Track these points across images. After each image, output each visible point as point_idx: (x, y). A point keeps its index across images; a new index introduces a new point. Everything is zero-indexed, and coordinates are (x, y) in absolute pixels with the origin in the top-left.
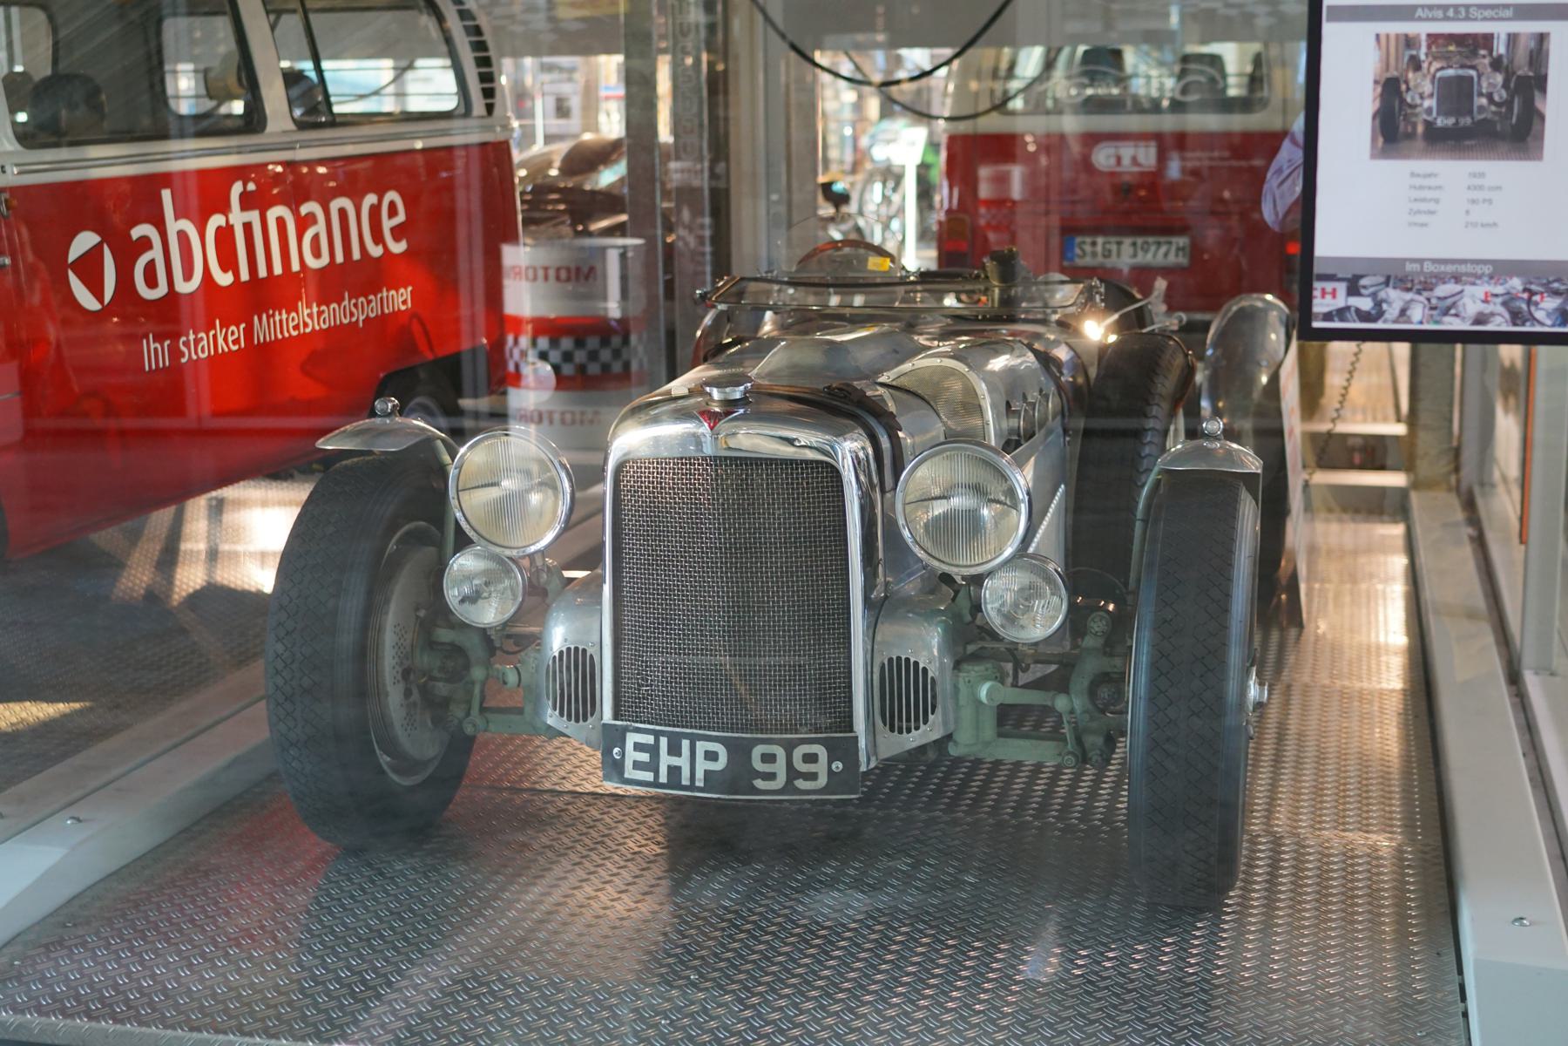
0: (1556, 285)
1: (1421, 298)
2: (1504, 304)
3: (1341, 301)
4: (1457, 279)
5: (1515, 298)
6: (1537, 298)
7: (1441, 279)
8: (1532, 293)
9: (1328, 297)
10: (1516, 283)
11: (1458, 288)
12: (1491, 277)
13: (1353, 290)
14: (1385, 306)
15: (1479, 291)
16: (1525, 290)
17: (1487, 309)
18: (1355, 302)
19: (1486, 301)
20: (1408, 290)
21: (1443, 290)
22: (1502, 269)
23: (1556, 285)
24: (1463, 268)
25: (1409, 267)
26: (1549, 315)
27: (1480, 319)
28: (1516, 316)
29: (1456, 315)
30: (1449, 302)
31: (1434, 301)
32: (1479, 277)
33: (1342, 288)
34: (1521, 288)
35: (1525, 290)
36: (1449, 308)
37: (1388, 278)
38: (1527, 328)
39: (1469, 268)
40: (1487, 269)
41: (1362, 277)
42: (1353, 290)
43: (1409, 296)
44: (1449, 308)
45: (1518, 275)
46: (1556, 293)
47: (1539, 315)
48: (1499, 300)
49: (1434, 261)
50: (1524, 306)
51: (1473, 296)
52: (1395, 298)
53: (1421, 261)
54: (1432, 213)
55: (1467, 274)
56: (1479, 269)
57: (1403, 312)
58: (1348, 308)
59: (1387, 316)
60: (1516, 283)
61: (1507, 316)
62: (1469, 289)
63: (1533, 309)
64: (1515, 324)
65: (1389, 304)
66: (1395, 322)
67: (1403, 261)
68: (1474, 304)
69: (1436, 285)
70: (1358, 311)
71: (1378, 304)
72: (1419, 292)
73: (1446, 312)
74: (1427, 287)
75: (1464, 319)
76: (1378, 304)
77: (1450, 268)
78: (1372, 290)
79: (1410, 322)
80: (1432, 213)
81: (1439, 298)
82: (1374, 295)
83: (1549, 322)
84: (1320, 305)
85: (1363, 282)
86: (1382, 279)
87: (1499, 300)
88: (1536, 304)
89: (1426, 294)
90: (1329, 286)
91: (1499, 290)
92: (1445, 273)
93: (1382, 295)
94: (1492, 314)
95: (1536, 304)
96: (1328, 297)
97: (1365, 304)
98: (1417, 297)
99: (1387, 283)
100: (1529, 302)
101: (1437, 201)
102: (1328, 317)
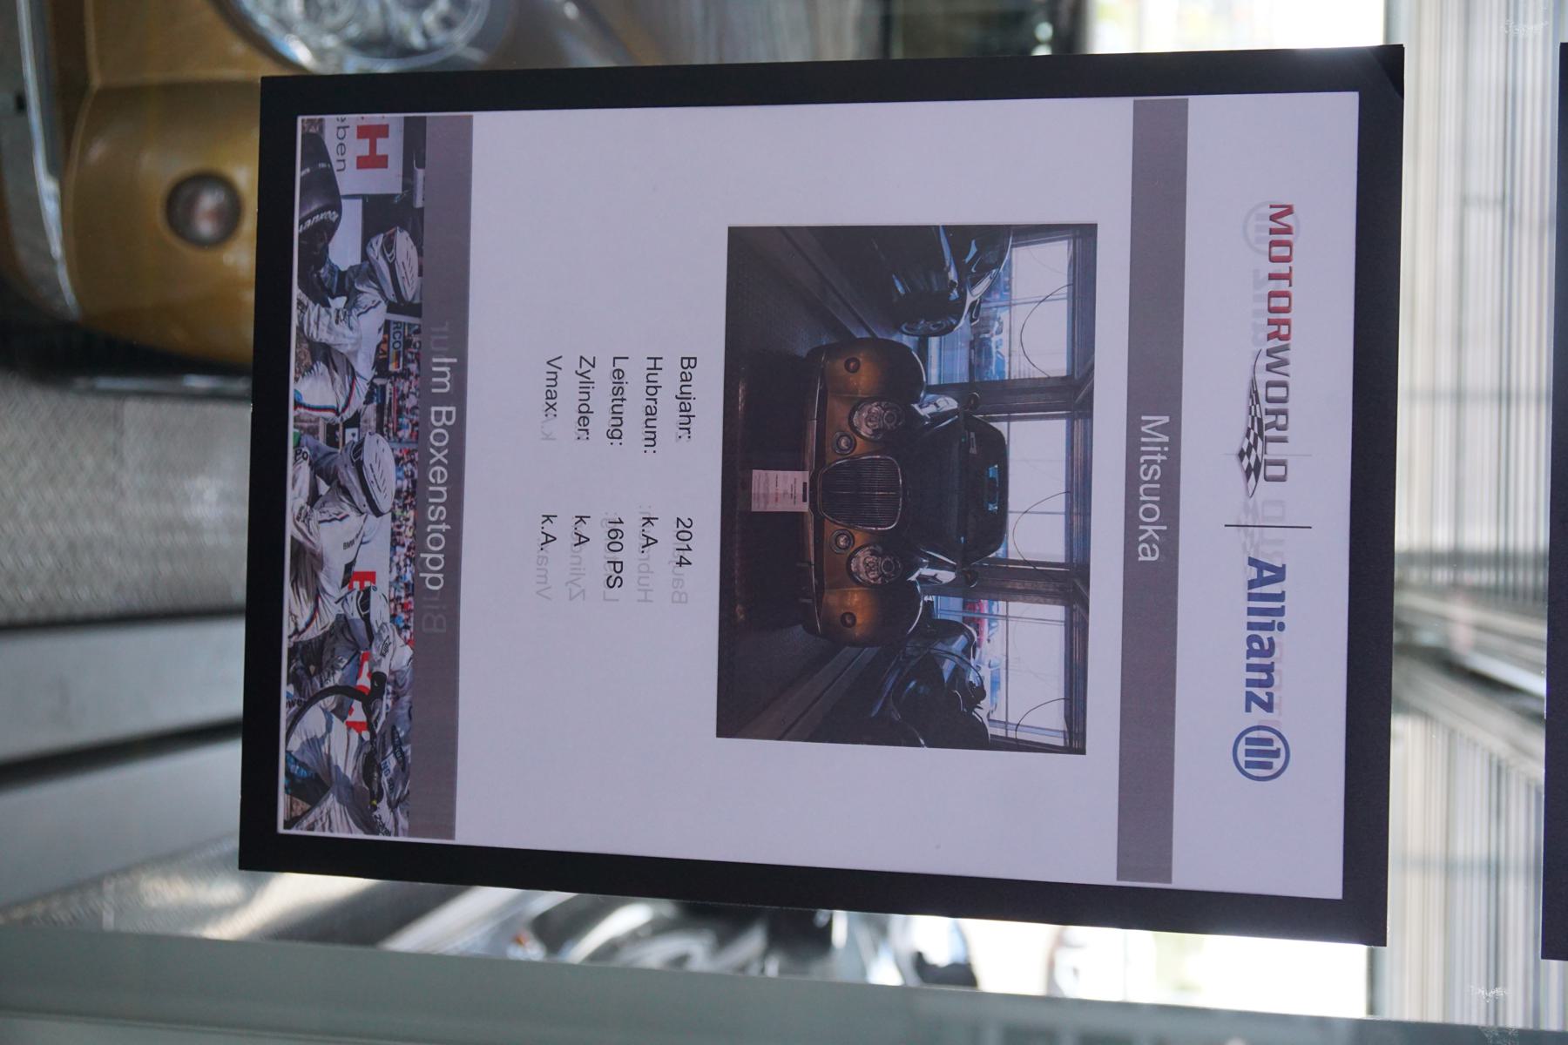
0: (392, 762)
1: (358, 402)
2: (343, 623)
3: (351, 180)
4: (412, 496)
5: (359, 654)
6: (358, 714)
7: (412, 457)
8: (369, 699)
9: (363, 148)
10: (398, 656)
13: (382, 216)
14: (340, 302)
15: (377, 558)
16: (378, 678)
17: (331, 581)
20: (381, 366)
21: (381, 456)
22: (433, 613)
24: (436, 511)
25: (441, 364)
26: (314, 743)
27: (309, 561)
28: (313, 655)
29: (314, 497)
30: (350, 478)
31: (350, 435)
33: (387, 181)
34: (384, 668)
35: (378, 678)
37: (414, 309)
38: (286, 689)
39: (437, 529)
40: (433, 577)
41: (417, 239)
42: (382, 216)
46: (370, 763)
47: (314, 720)
48: (354, 613)
49: (457, 433)
50: (336, 679)
52: (360, 331)
53: (458, 396)
54: (584, 417)
55: (420, 525)
56: (433, 553)
57: (324, 354)
59: (314, 310)
60: (398, 656)
61: (311, 634)
63: (330, 702)
64: (292, 651)
65: (343, 316)
66: (300, 329)
67: (458, 345)
68: (346, 539)
70: (329, 229)
71: (345, 285)
73: (318, 470)
74: (388, 415)
75: (304, 517)
76: (345, 285)
77: (438, 475)
78: (382, 265)
79: (296, 380)
80: (584, 417)
81: (358, 448)
82: (366, 271)
83: (296, 744)
84: (340, 134)
85: (403, 241)
86: (409, 293)
87: (354, 613)
88: (341, 712)
89: (370, 412)
90: (392, 146)
91: (380, 611)
92: (424, 466)
93: (369, 295)
94: (317, 595)
96: (363, 148)
97: (344, 250)
98: (362, 387)
100: (348, 691)
101: (615, 434)
102: (316, 148)
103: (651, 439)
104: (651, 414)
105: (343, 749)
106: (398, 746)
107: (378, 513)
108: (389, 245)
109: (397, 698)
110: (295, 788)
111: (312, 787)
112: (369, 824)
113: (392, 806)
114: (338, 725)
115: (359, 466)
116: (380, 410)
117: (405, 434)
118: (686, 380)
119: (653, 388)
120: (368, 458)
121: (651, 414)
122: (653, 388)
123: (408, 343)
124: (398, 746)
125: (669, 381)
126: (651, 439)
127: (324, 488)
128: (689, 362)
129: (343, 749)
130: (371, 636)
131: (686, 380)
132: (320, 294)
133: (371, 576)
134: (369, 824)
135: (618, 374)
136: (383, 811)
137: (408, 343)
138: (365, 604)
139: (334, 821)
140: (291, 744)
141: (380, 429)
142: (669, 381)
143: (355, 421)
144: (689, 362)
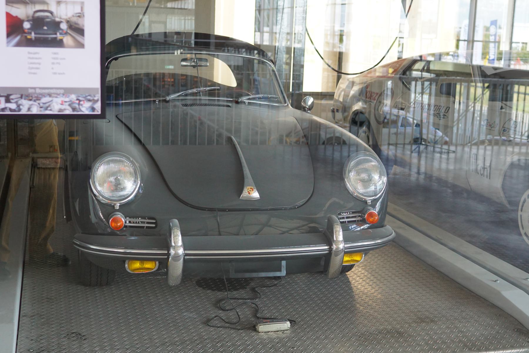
1: (36, 103)
2: (70, 105)
4: (50, 95)
5: (73, 103)
6: (82, 103)
7: (44, 95)
8: (80, 101)
10: (73, 97)
11: (50, 99)
12: (63, 95)
14: (21, 107)
15: (59, 100)
16: (77, 99)
17: (63, 107)
18: (9, 105)
19: (62, 104)
20: (31, 100)
21: (44, 100)
23: (89, 97)
26: (87, 109)
28: (74, 109)
29: (51, 110)
30: (47, 105)
32: (59, 95)
34: (75, 99)
35: (77, 99)
36: (47, 107)
41: (11, 95)
42: (8, 100)
43: (31, 102)
44: (47, 107)
45: (74, 93)
46: (89, 100)
47: (83, 109)
48: (67, 103)
50: (77, 106)
51: (57, 103)
57: (29, 109)
58: (6, 108)
59: (22, 111)
60: (73, 97)
62: (55, 100)
63: (81, 107)
67: (27, 89)
69: (41, 98)
71: (18, 106)
72: (35, 101)
73: (46, 109)
74: (38, 99)
76: (18, 106)
78: (16, 100)
81: (43, 103)
82: (16, 102)
85: (11, 97)
86: (19, 96)
87: (67, 103)
88: (82, 105)
89: (38, 102)
92: (45, 93)
93: (20, 102)
94: (65, 109)
95: (82, 105)
97: (13, 106)
99: (21, 97)
100: (79, 104)
103: (40, 58)
104: (36, 58)
105: (88, 105)
106: (86, 96)
107: (52, 101)
108: (12, 99)
109: (79, 97)
110: (93, 111)
111: (93, 109)
112: (98, 100)
113: (95, 97)
114: (84, 105)
115: (46, 103)
116: (37, 100)
117: (41, 96)
118: (31, 53)
119: (33, 58)
120: (44, 102)
121: (36, 58)
122: (33, 58)
123: (27, 96)
124: (86, 96)
125: (32, 56)
126: (40, 58)
127: (49, 109)
128: (29, 53)
129: (88, 105)
130: (71, 101)
131: (31, 53)
132: (20, 110)
133: (62, 101)
134: (98, 100)
135: (31, 63)
136: (96, 98)
137: (27, 96)
138: (66, 102)
139: (98, 106)
140: (87, 112)
141: (40, 100)
142: (32, 56)
143: (39, 104)
144: (29, 53)
